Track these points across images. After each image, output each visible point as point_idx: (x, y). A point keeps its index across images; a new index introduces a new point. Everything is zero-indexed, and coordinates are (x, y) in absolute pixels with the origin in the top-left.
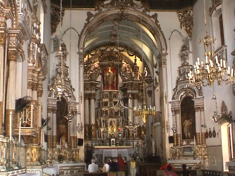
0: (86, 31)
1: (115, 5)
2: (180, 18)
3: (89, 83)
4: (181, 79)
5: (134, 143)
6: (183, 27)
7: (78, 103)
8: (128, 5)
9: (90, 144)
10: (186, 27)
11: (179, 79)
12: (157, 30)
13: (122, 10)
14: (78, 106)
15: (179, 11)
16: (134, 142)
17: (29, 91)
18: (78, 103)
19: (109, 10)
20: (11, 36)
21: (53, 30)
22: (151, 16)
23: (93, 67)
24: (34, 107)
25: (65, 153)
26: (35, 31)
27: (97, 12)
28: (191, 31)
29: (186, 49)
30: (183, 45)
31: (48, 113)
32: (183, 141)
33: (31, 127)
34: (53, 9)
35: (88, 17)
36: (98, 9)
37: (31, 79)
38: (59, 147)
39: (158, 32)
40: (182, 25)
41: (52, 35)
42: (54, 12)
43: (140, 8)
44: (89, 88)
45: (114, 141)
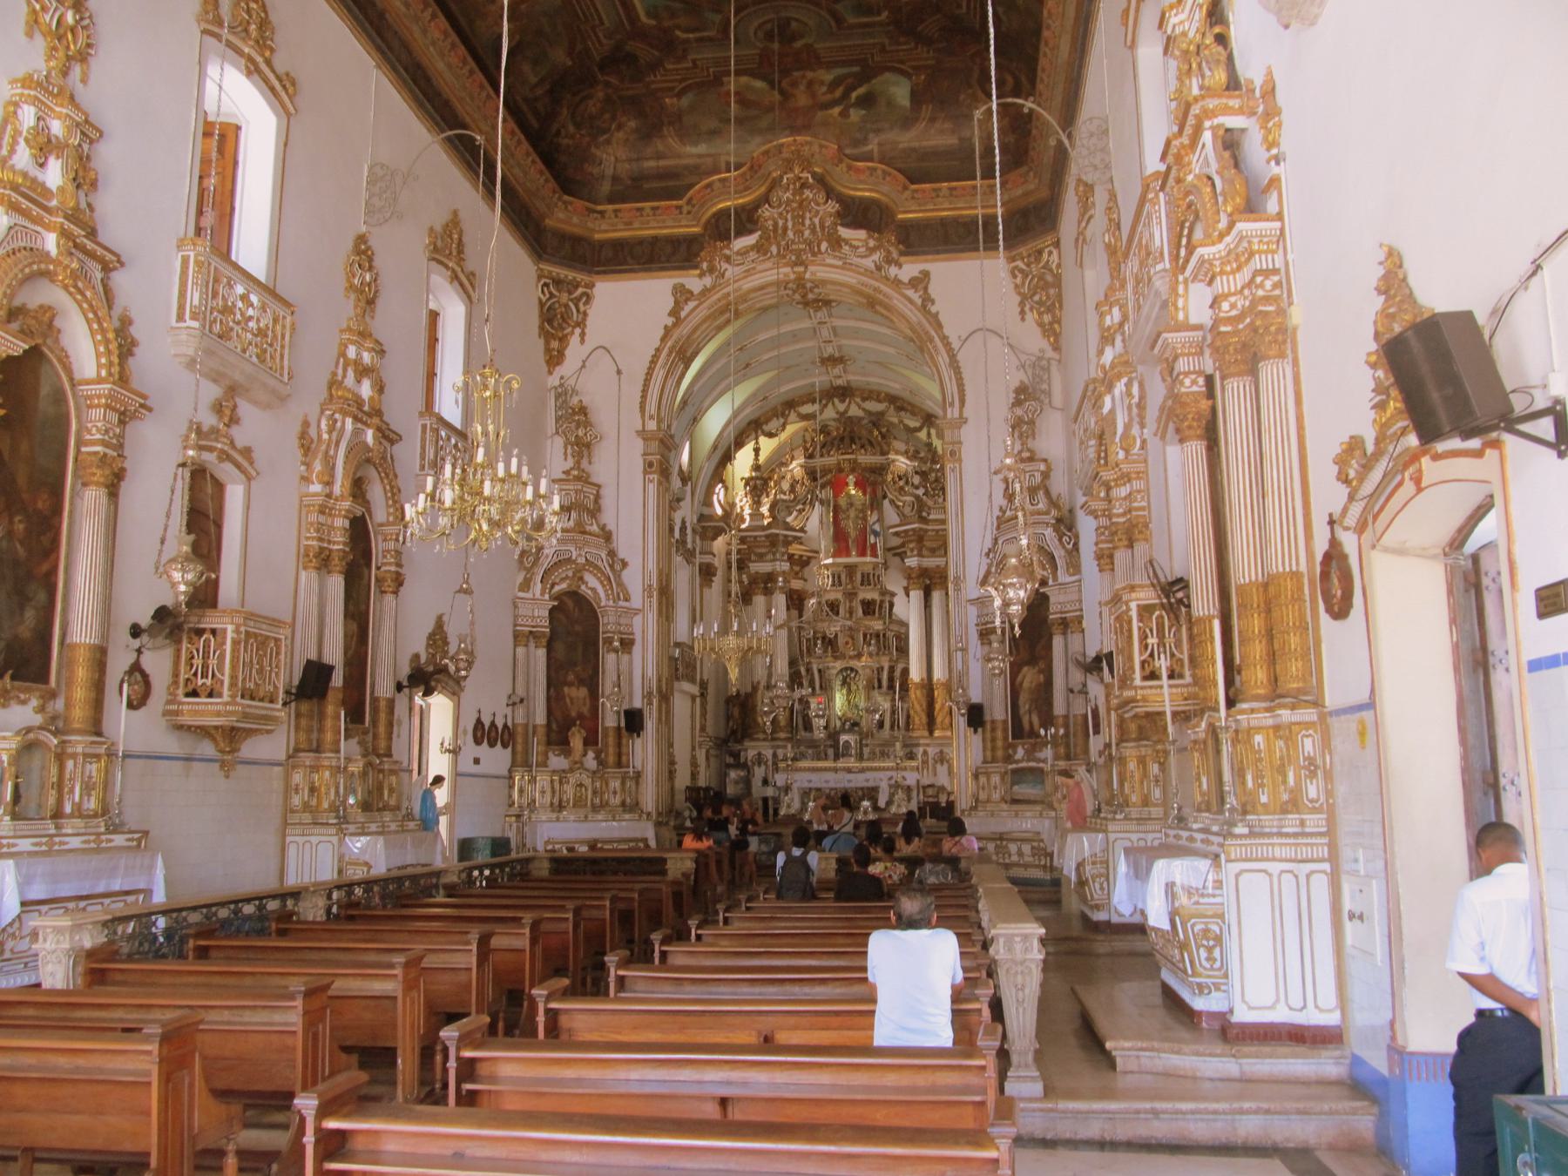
0: (670, 353)
1: (774, 249)
2: (1019, 280)
3: (766, 536)
4: (1008, 513)
6: (1029, 316)
7: (637, 612)
8: (819, 246)
9: (768, 753)
10: (1040, 314)
11: (1004, 512)
12: (927, 333)
13: (796, 269)
14: (637, 620)
15: (1014, 253)
17: (308, 578)
18: (637, 612)
19: (748, 273)
20: (90, 407)
21: (554, 359)
22: (906, 281)
23: (789, 476)
24: (237, 631)
25: (581, 785)
26: (351, 373)
27: (708, 281)
28: (1056, 326)
29: (1025, 400)
30: (1017, 384)
31: (515, 646)
32: (1014, 747)
33: (226, 698)
34: (546, 285)
35: (676, 302)
36: (711, 270)
37: (313, 538)
38: (557, 761)
39: (931, 340)
40: (1027, 309)
41: (550, 373)
42: (551, 293)
43: (865, 256)
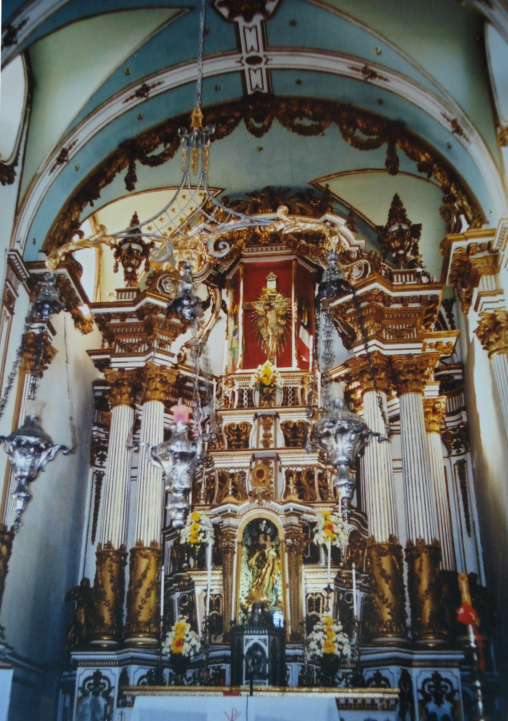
5: (414, 672)
16: (409, 663)
44: (139, 344)
45: (266, 649)
